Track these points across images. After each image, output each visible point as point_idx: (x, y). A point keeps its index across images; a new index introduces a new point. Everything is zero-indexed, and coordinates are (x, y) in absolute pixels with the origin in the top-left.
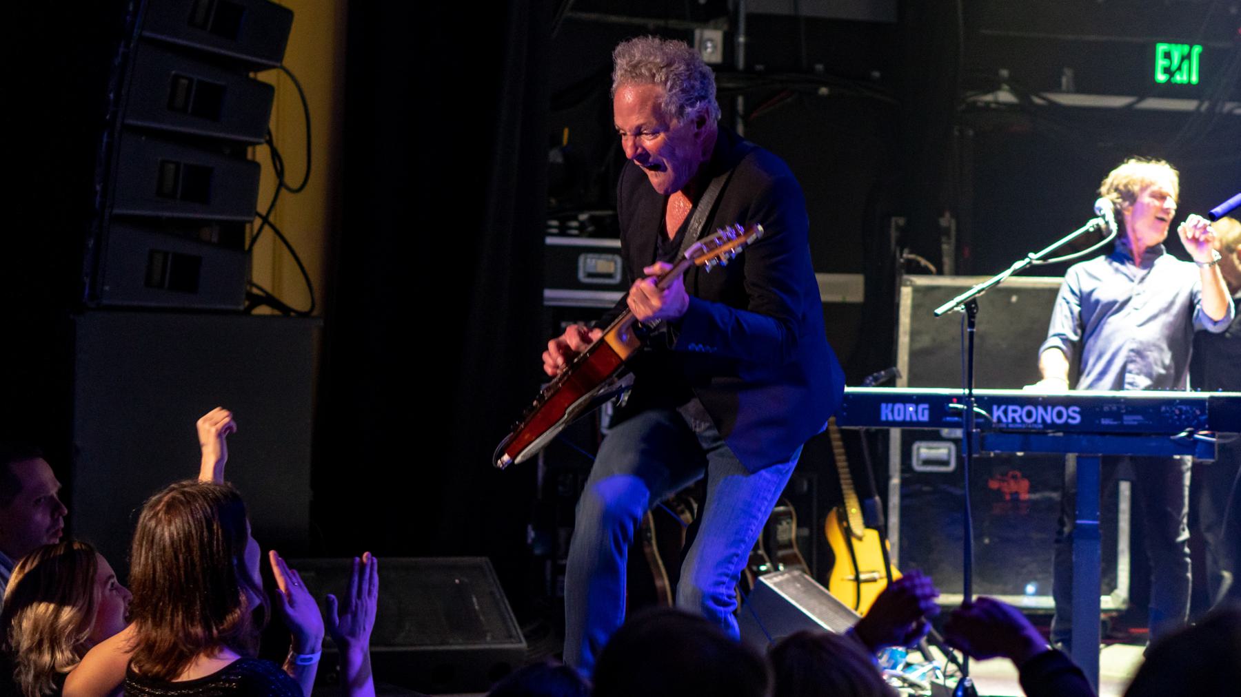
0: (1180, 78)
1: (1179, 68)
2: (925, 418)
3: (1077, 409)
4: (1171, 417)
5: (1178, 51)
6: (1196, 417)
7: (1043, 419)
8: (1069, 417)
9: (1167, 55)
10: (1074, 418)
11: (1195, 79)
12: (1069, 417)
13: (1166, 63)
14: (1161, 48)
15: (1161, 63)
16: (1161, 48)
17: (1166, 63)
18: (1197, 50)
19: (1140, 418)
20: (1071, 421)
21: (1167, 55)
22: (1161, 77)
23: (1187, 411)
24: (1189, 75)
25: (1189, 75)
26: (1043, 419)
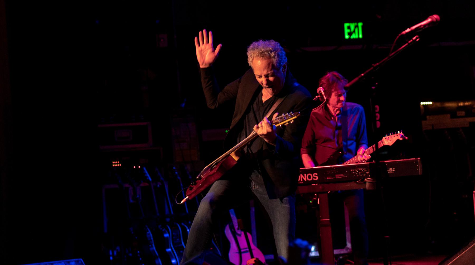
0: (354, 36)
1: (354, 31)
2: (458, 113)
3: (317, 174)
4: (355, 174)
5: (352, 26)
6: (365, 172)
7: (303, 179)
8: (313, 177)
9: (349, 28)
10: (316, 178)
11: (361, 36)
12: (313, 177)
13: (349, 31)
14: (346, 25)
15: (347, 31)
16: (346, 25)
17: (349, 31)
18: (360, 24)
19: (342, 175)
20: (314, 179)
21: (349, 28)
22: (347, 37)
23: (361, 171)
24: (358, 35)
25: (358, 35)
26: (303, 179)
